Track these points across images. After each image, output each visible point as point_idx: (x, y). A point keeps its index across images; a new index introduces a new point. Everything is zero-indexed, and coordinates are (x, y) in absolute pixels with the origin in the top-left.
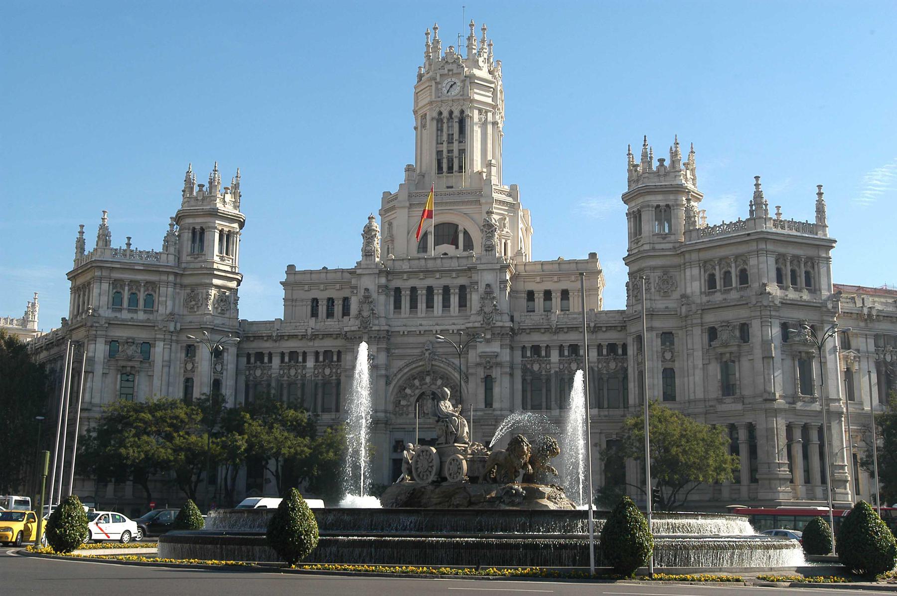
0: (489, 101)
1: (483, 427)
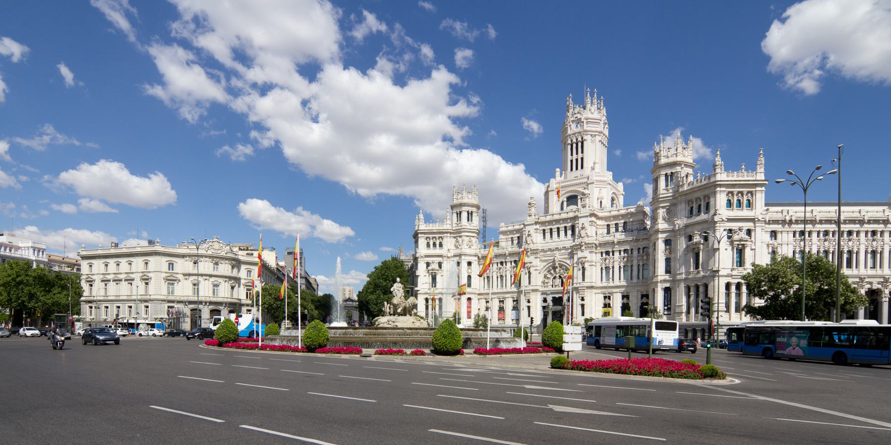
0: (598, 130)
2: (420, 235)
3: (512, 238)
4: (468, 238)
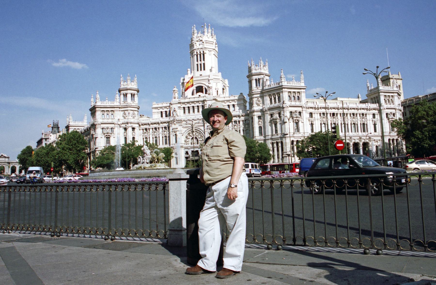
2: (97, 109)
4: (132, 112)
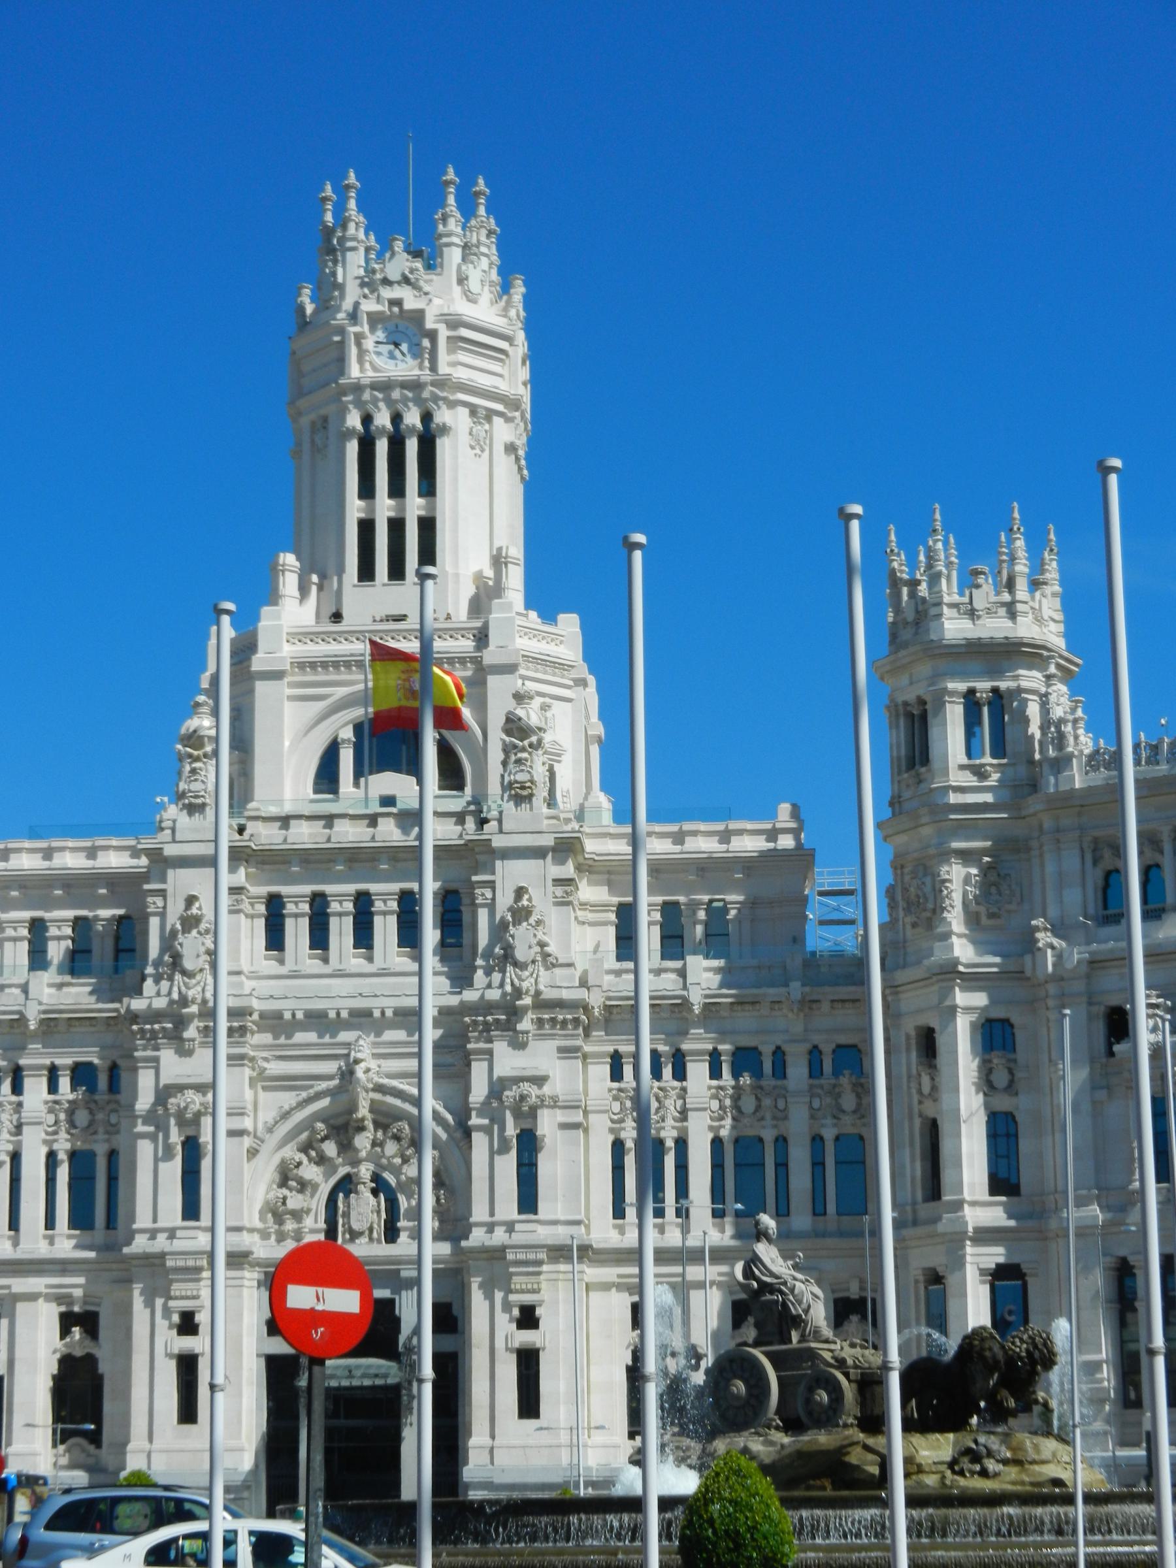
1: (511, 1270)
3: (37, 928)
